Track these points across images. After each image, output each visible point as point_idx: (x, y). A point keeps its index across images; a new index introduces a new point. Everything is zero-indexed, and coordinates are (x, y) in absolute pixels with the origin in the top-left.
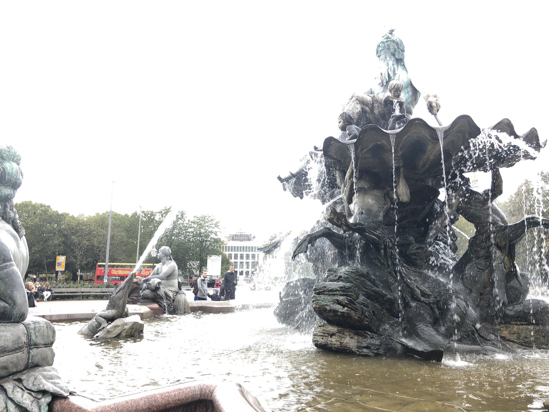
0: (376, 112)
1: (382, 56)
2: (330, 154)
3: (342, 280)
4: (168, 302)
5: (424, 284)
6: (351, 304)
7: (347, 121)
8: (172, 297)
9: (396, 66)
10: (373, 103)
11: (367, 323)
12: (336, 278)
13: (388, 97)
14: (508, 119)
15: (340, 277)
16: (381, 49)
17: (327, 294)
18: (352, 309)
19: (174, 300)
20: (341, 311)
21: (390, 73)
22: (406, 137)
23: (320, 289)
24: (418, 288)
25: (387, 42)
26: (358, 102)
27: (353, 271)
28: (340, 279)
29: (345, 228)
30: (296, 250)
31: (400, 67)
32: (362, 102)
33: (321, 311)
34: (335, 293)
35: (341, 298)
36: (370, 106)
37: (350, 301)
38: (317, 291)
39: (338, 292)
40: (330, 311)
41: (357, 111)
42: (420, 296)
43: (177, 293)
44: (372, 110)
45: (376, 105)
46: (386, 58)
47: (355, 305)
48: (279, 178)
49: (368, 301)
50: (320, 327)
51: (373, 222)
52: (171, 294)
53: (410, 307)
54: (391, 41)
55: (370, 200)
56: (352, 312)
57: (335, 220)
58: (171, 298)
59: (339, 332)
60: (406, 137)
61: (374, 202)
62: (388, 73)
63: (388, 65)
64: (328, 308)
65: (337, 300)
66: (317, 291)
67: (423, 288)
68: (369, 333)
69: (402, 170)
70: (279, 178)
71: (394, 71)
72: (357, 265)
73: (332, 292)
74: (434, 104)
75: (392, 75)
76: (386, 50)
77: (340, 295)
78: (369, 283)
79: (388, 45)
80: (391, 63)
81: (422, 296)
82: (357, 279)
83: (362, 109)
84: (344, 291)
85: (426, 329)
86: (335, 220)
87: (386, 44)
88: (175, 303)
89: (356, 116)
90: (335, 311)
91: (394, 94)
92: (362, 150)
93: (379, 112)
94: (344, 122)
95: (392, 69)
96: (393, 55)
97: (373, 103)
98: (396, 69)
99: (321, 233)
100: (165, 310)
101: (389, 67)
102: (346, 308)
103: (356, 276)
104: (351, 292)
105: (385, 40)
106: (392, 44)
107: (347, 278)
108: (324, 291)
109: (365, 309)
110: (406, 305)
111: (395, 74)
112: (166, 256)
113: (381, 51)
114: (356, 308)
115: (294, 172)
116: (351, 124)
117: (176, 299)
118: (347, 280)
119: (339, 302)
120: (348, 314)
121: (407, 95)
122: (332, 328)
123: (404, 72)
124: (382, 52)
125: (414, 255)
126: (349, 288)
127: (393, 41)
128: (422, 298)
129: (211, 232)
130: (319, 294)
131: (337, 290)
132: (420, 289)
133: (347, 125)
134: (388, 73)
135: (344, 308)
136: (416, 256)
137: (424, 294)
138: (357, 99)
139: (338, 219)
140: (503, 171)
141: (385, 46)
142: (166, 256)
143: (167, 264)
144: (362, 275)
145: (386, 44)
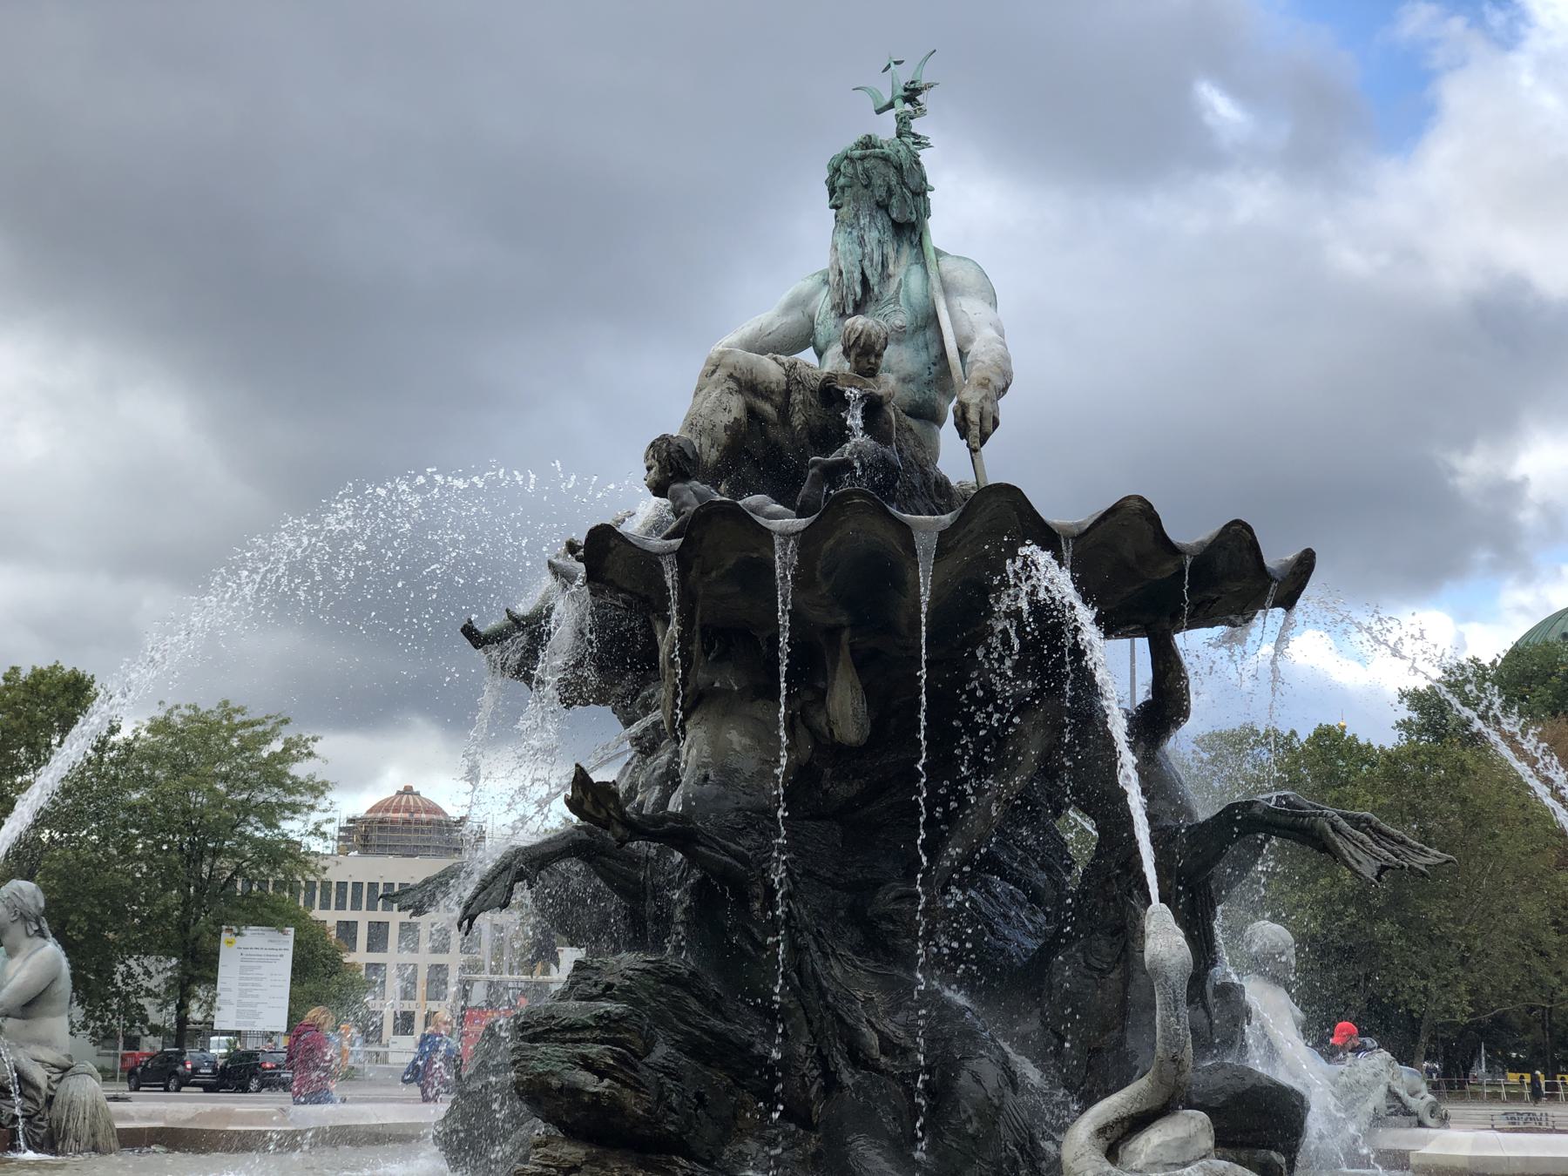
0: (797, 420)
1: (844, 209)
2: (609, 576)
3: (614, 998)
4: (28, 1104)
5: (896, 1013)
6: (625, 1067)
7: (671, 466)
8: (43, 1084)
9: (890, 250)
10: (788, 393)
11: (672, 1128)
12: (595, 991)
13: (830, 378)
14: (1141, 499)
15: (610, 986)
16: (842, 181)
17: (556, 1040)
18: (625, 1084)
19: (50, 1100)
20: (592, 1089)
21: (868, 272)
22: (832, 542)
23: (539, 1024)
24: (872, 1026)
25: (862, 158)
26: (732, 385)
27: (649, 966)
28: (608, 992)
29: (619, 830)
30: (474, 898)
31: (906, 249)
32: (748, 386)
33: (537, 1094)
34: (581, 1035)
35: (593, 1050)
36: (778, 399)
37: (621, 1059)
38: (530, 1031)
39: (588, 1035)
40: (561, 1090)
41: (725, 419)
42: (875, 1053)
43: (65, 1070)
44: (784, 410)
45: (797, 397)
46: (856, 216)
47: (636, 1071)
48: (469, 632)
49: (684, 1061)
50: (536, 1146)
51: (739, 810)
52: (39, 1075)
53: (841, 1087)
54: (876, 157)
55: (735, 738)
56: (627, 1092)
57: (587, 807)
58: (37, 1089)
59: (591, 1160)
60: (832, 542)
61: (746, 741)
62: (863, 273)
63: (862, 242)
64: (555, 1082)
65: (584, 1057)
66: (530, 1031)
67: (888, 1026)
68: (682, 1162)
69: (845, 636)
70: (469, 632)
71: (884, 265)
72: (678, 955)
73: (567, 1032)
74: (973, 415)
75: (873, 280)
76: (858, 188)
77: (595, 1041)
78: (694, 1005)
79: (865, 170)
80: (872, 236)
81: (883, 1052)
82: (660, 993)
83: (751, 412)
84: (606, 1023)
85: (872, 1154)
86: (587, 807)
87: (860, 168)
88: (57, 1111)
89: (723, 437)
90: (574, 1091)
91: (857, 362)
92: (705, 573)
93: (806, 422)
94: (662, 470)
95: (877, 257)
96: (883, 207)
97: (788, 393)
98: (891, 262)
99: (563, 844)
100: (15, 1131)
101: (867, 250)
102: (607, 1082)
103: (657, 982)
104: (628, 1030)
105: (857, 153)
106: (881, 164)
107: (629, 990)
108: (551, 1030)
109: (670, 1084)
110: (831, 1083)
111: (885, 277)
112: (24, 918)
113: (843, 188)
114: (639, 1082)
115: (523, 609)
116: (685, 477)
117: (59, 1097)
118: (626, 994)
119: (588, 1065)
120: (611, 1097)
121: (924, 356)
122: (572, 1149)
123: (916, 271)
124: (848, 192)
125: (889, 918)
126: (622, 1018)
127: (885, 159)
128: (883, 1059)
129: (246, 809)
130: (534, 1038)
131: (586, 1027)
132: (877, 1031)
133: (674, 479)
134: (863, 273)
135: (601, 1079)
136: (894, 922)
137: (888, 1046)
138: (731, 376)
139: (597, 803)
140: (1192, 643)
141: (856, 174)
142: (24, 918)
143: (24, 951)
144: (675, 980)
145: (860, 168)
